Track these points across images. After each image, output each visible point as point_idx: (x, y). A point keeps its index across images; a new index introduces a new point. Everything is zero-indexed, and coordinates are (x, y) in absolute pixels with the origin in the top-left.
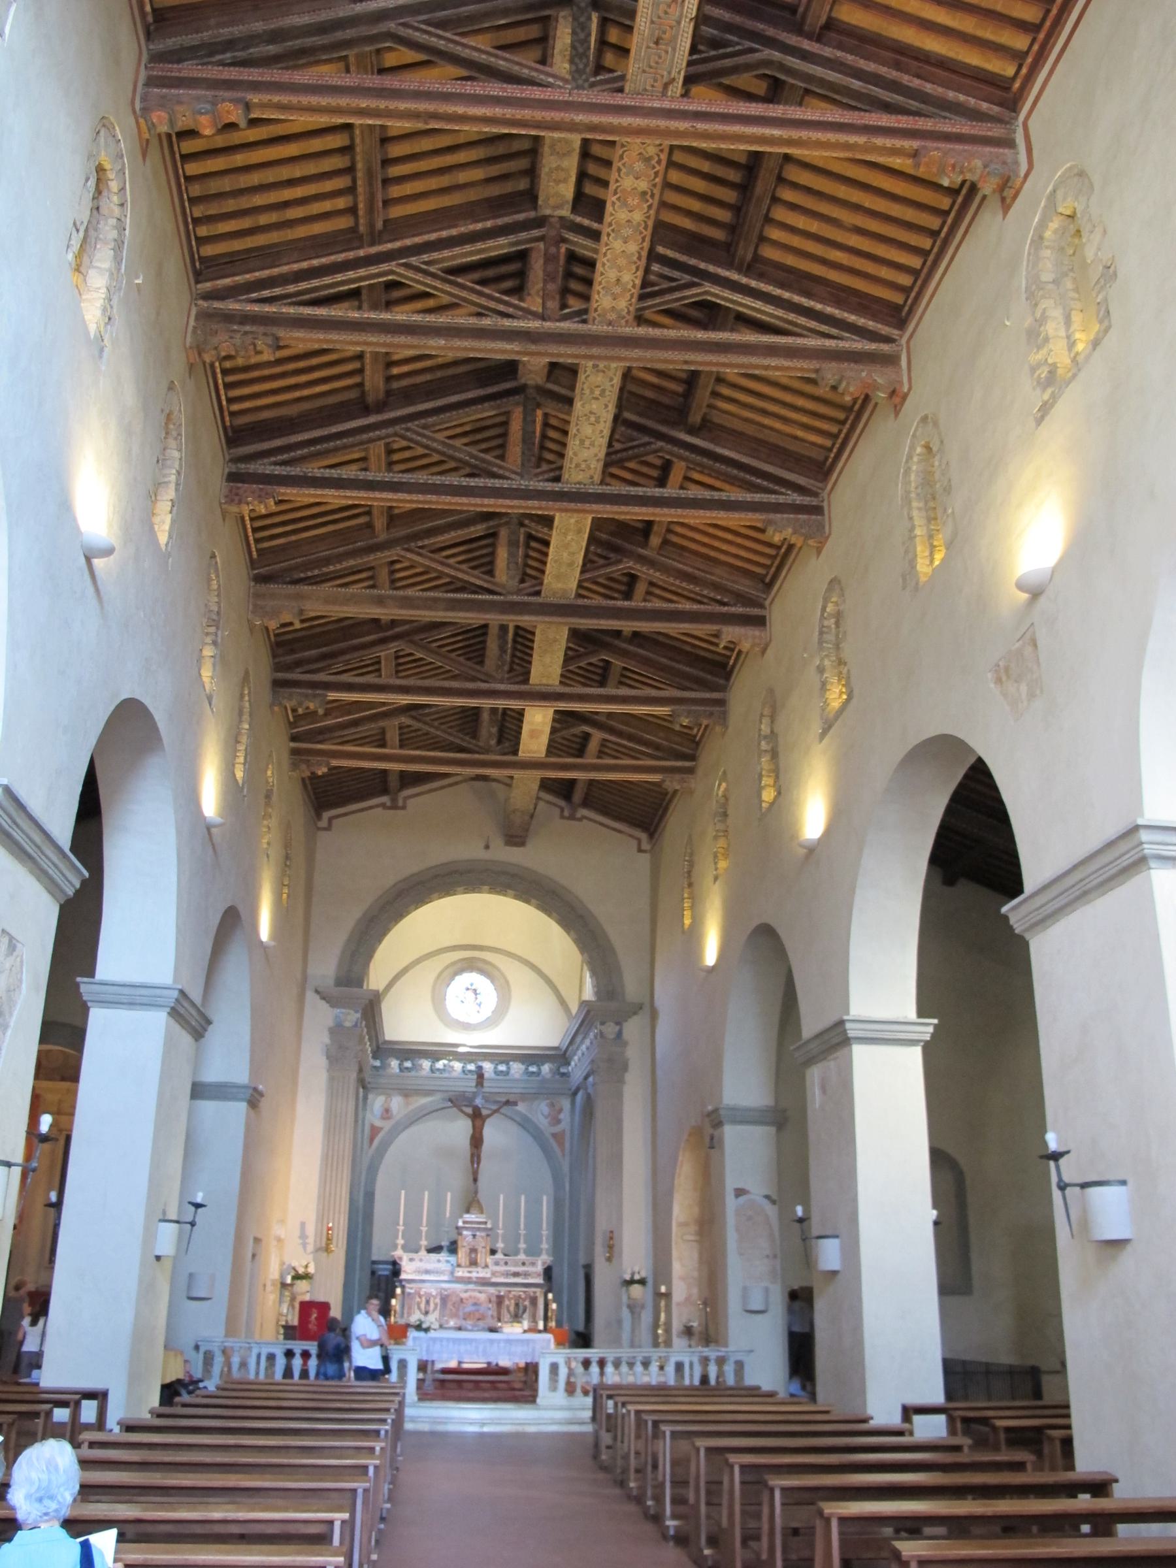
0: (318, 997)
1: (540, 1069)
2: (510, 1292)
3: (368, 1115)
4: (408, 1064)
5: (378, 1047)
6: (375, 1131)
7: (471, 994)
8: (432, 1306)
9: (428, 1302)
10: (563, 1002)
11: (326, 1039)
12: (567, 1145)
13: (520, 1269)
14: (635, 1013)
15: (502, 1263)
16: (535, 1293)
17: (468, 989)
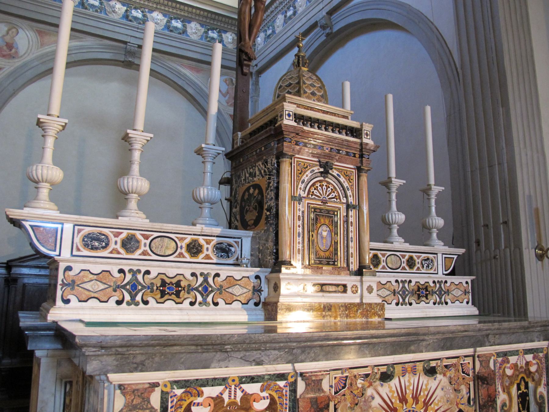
1: (220, 36)
2: (505, 354)
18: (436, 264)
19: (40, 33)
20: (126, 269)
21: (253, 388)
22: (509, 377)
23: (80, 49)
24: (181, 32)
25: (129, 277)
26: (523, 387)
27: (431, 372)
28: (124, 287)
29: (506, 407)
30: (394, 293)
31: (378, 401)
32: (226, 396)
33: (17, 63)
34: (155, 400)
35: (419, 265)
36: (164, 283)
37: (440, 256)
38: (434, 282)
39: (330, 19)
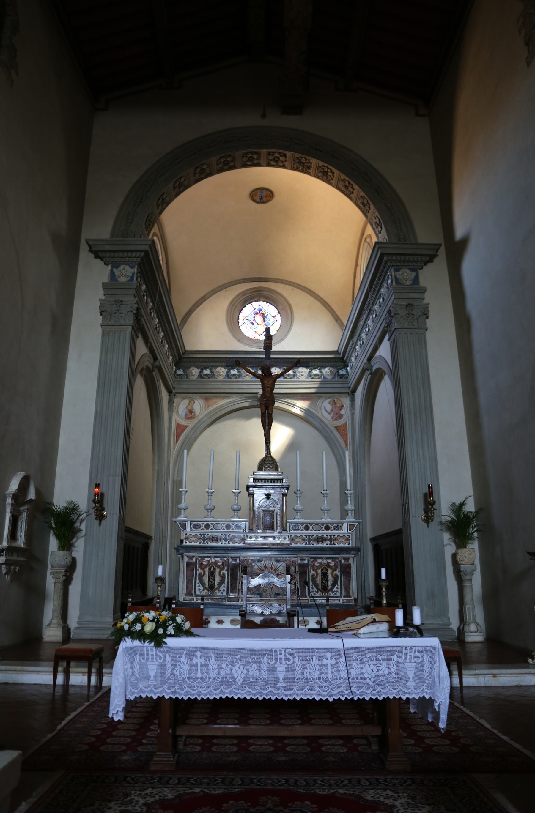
0: (92, 256)
2: (315, 559)
3: (175, 416)
4: (207, 372)
5: (180, 358)
6: (181, 428)
7: (259, 319)
8: (218, 579)
9: (212, 574)
10: (337, 319)
11: (100, 294)
12: (349, 435)
13: (325, 534)
14: (431, 260)
15: (302, 528)
16: (346, 559)
17: (257, 313)
18: (343, 528)
19: (206, 399)
20: (202, 534)
21: (218, 559)
22: (317, 566)
23: (230, 404)
24: (292, 376)
25: (202, 536)
26: (325, 571)
27: (278, 561)
28: (201, 539)
29: (314, 575)
30: (304, 540)
31: (256, 567)
32: (211, 560)
33: (196, 421)
34: (194, 560)
35: (332, 529)
36: (213, 537)
37: (346, 524)
38: (327, 536)
39: (370, 363)
